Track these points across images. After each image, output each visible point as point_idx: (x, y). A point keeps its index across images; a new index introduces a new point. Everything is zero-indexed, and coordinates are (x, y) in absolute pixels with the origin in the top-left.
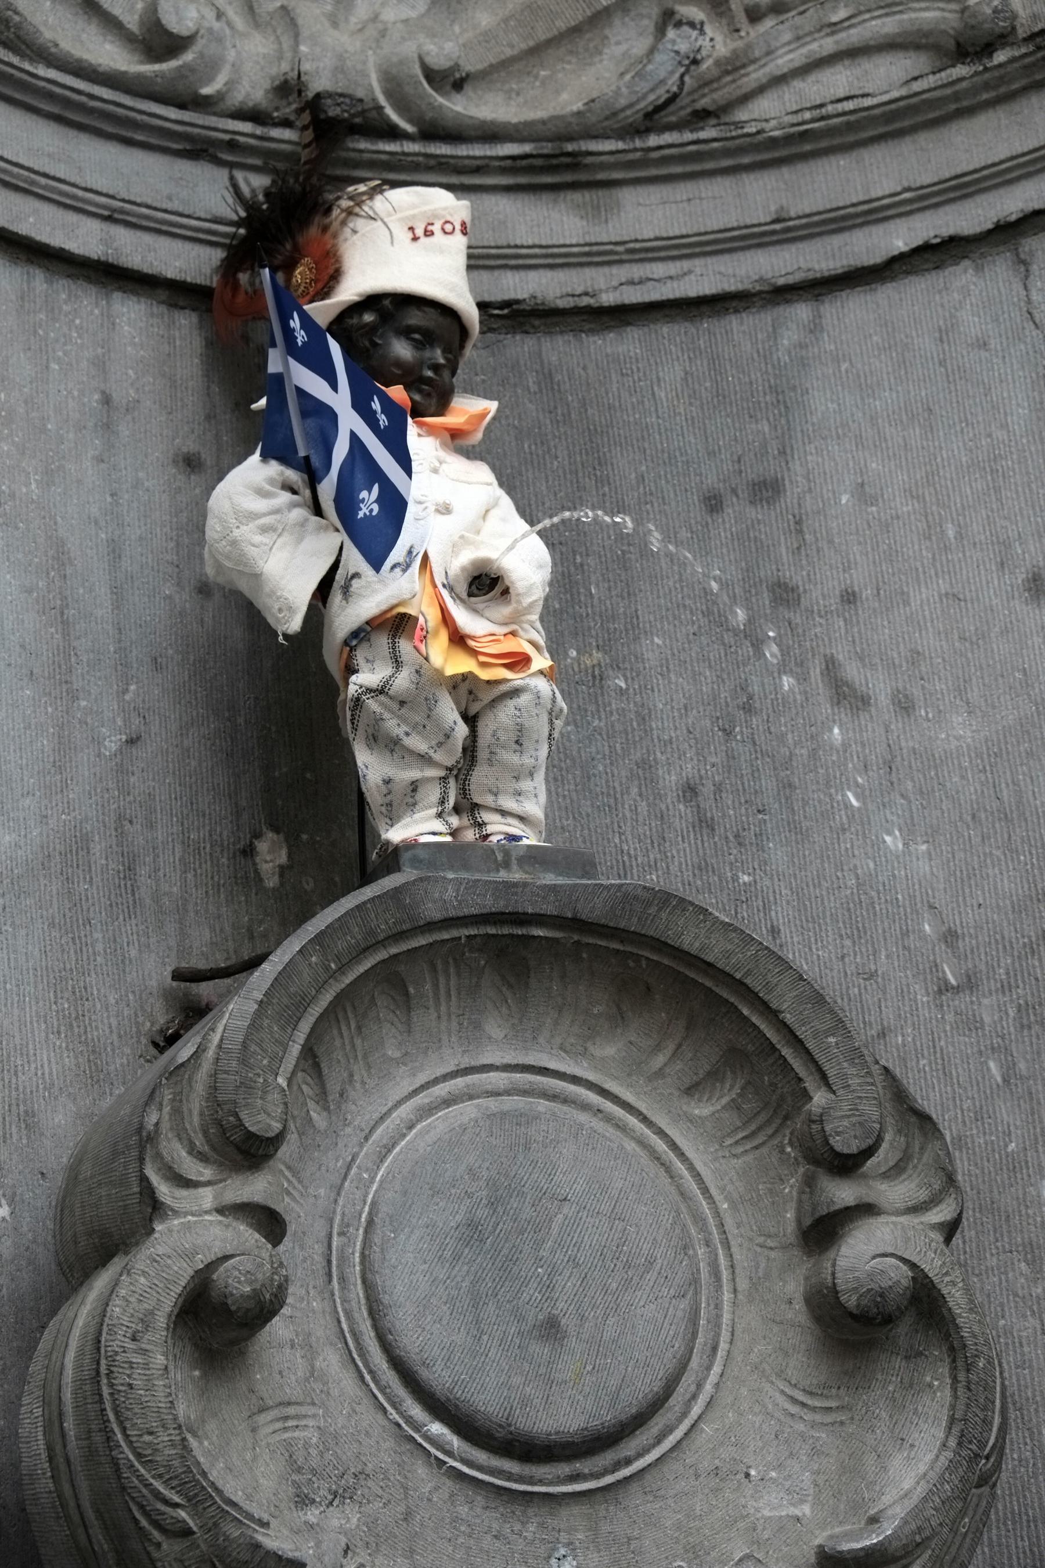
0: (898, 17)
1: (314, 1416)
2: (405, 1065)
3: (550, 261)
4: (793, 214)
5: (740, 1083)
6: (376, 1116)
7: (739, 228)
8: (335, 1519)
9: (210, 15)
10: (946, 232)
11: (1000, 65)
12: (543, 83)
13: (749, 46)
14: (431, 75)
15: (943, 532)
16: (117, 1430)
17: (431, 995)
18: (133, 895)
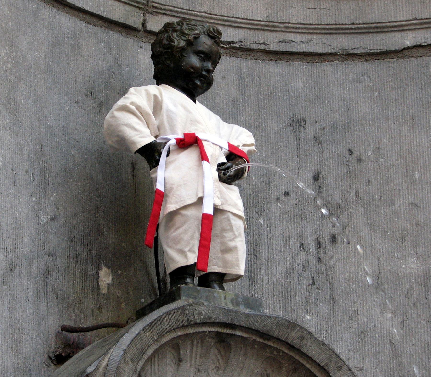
7: (336, 24)
15: (413, 175)
17: (189, 355)
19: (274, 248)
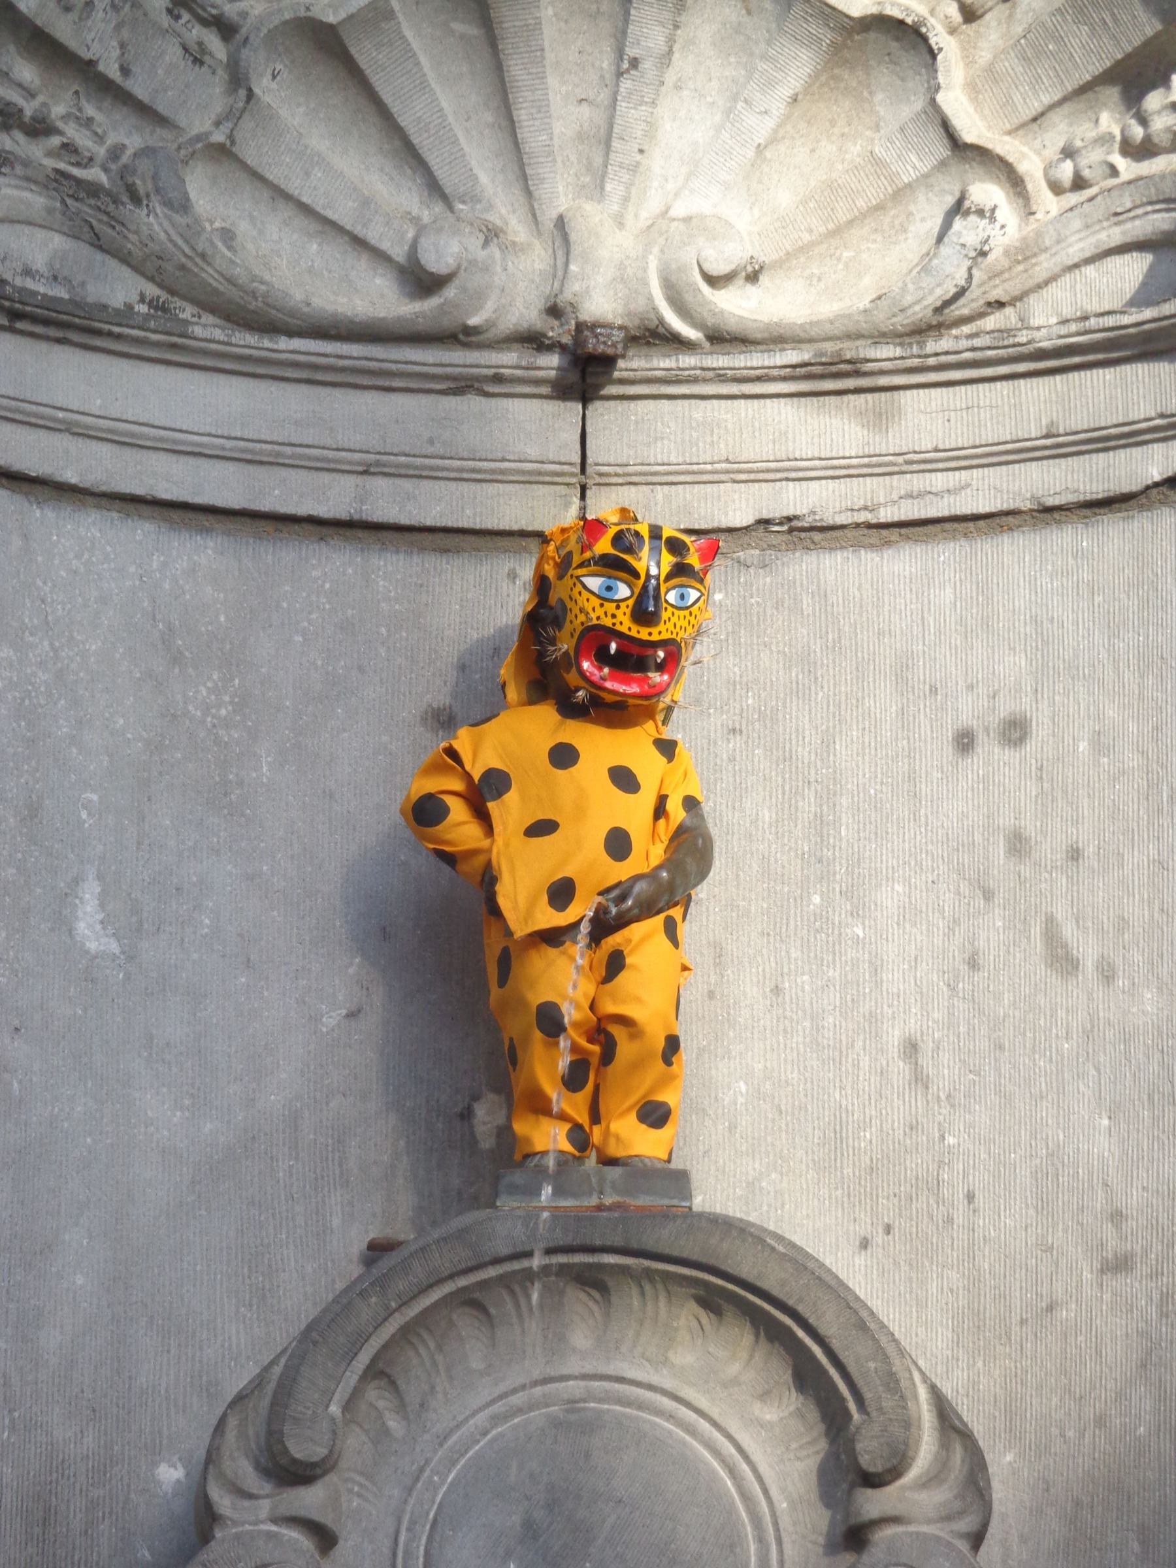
2: (489, 1375)
3: (830, 473)
4: (1061, 431)
12: (847, 266)
14: (712, 281)
17: (513, 1312)
18: (341, 1165)
19: (884, 989)
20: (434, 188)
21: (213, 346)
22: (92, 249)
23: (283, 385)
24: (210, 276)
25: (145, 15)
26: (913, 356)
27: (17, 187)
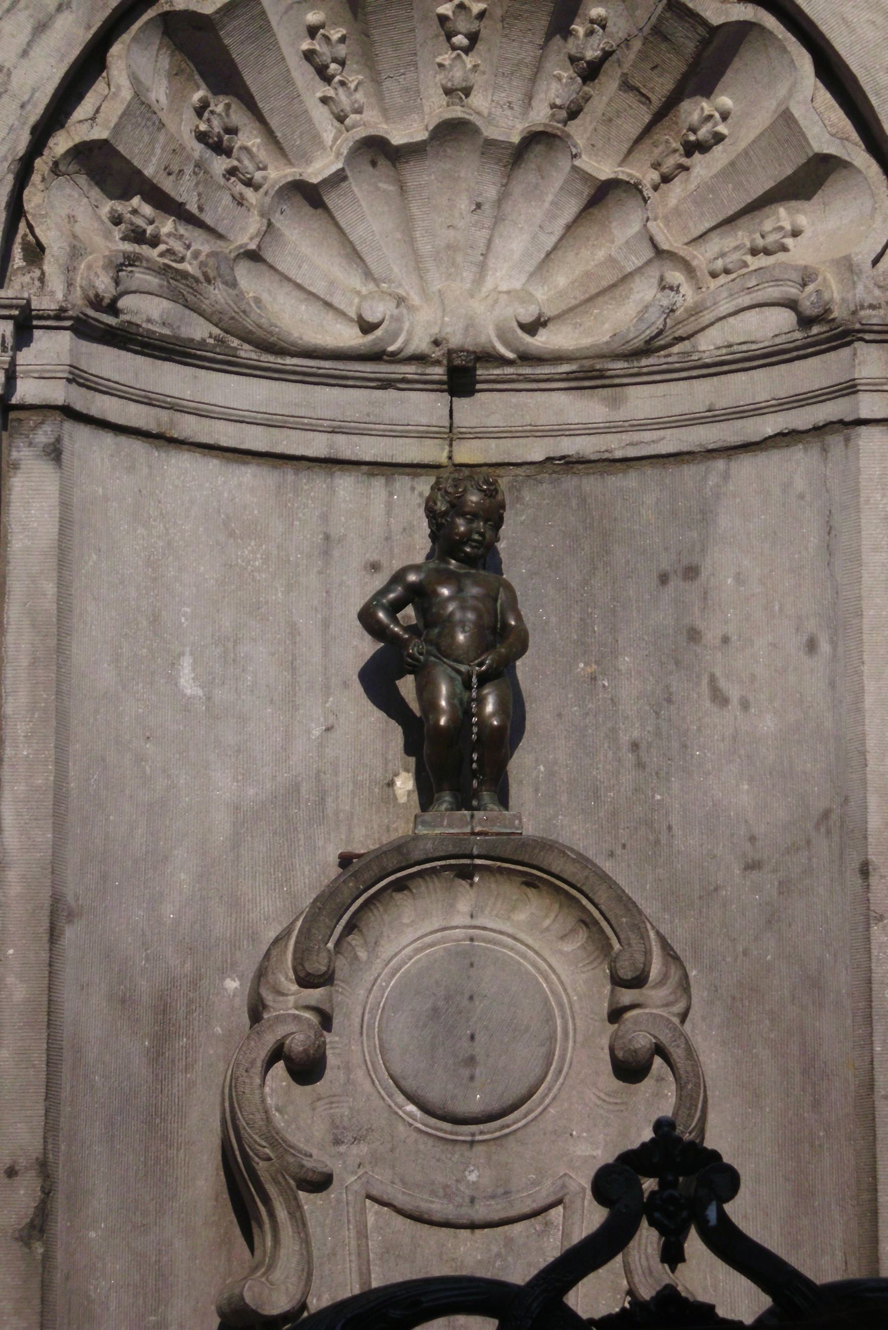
0: (781, 288)
1: (347, 1102)
5: (586, 936)
6: (393, 953)
8: (355, 1150)
9: (392, 305)
10: (792, 426)
11: (814, 336)
12: (595, 318)
13: (703, 300)
14: (523, 327)
16: (239, 1112)
20: (368, 274)
21: (251, 362)
22: (183, 308)
23: (287, 383)
24: (249, 324)
25: (211, 177)
26: (633, 367)
27: (143, 273)
